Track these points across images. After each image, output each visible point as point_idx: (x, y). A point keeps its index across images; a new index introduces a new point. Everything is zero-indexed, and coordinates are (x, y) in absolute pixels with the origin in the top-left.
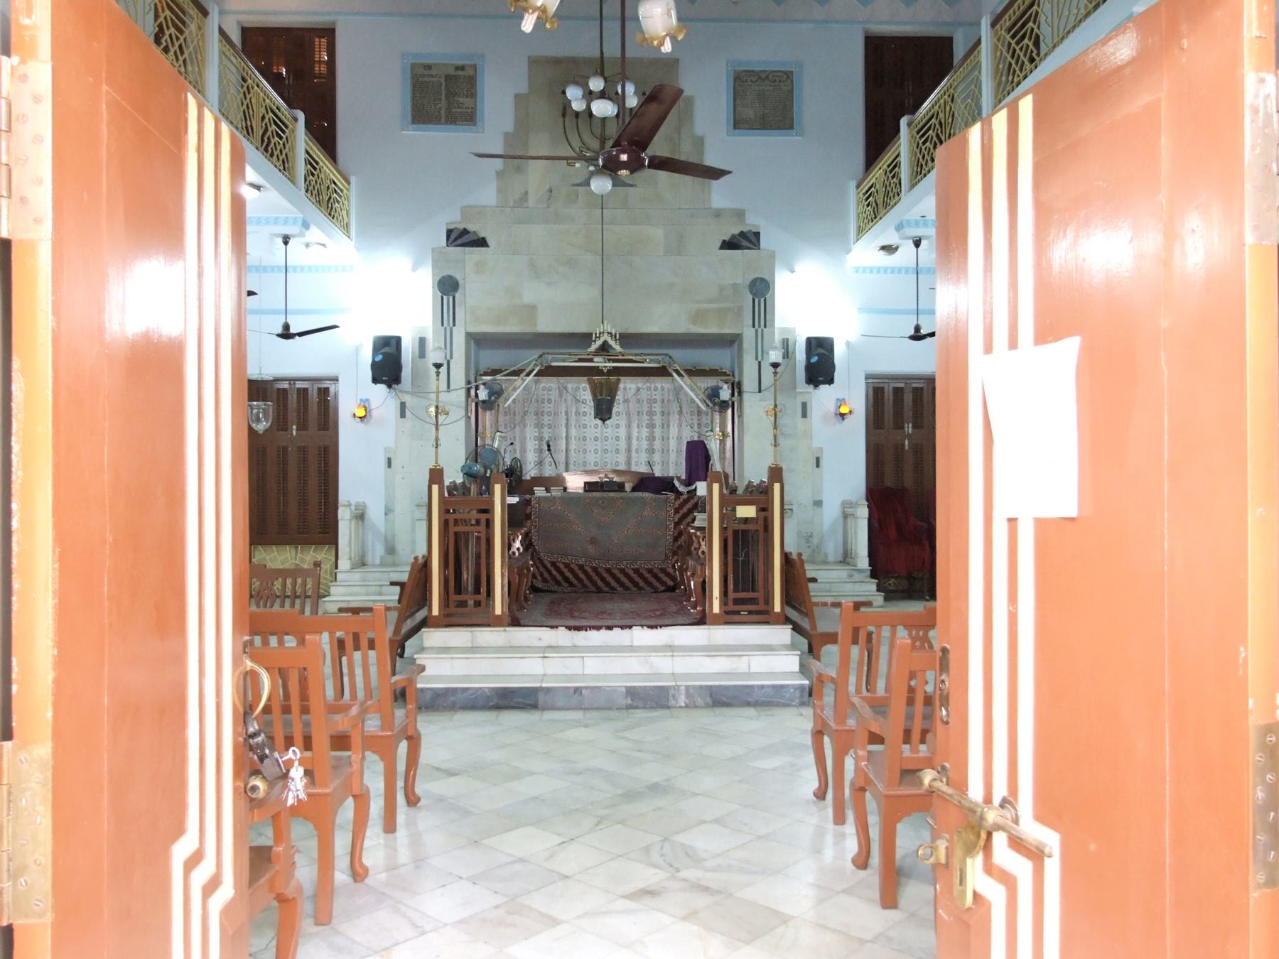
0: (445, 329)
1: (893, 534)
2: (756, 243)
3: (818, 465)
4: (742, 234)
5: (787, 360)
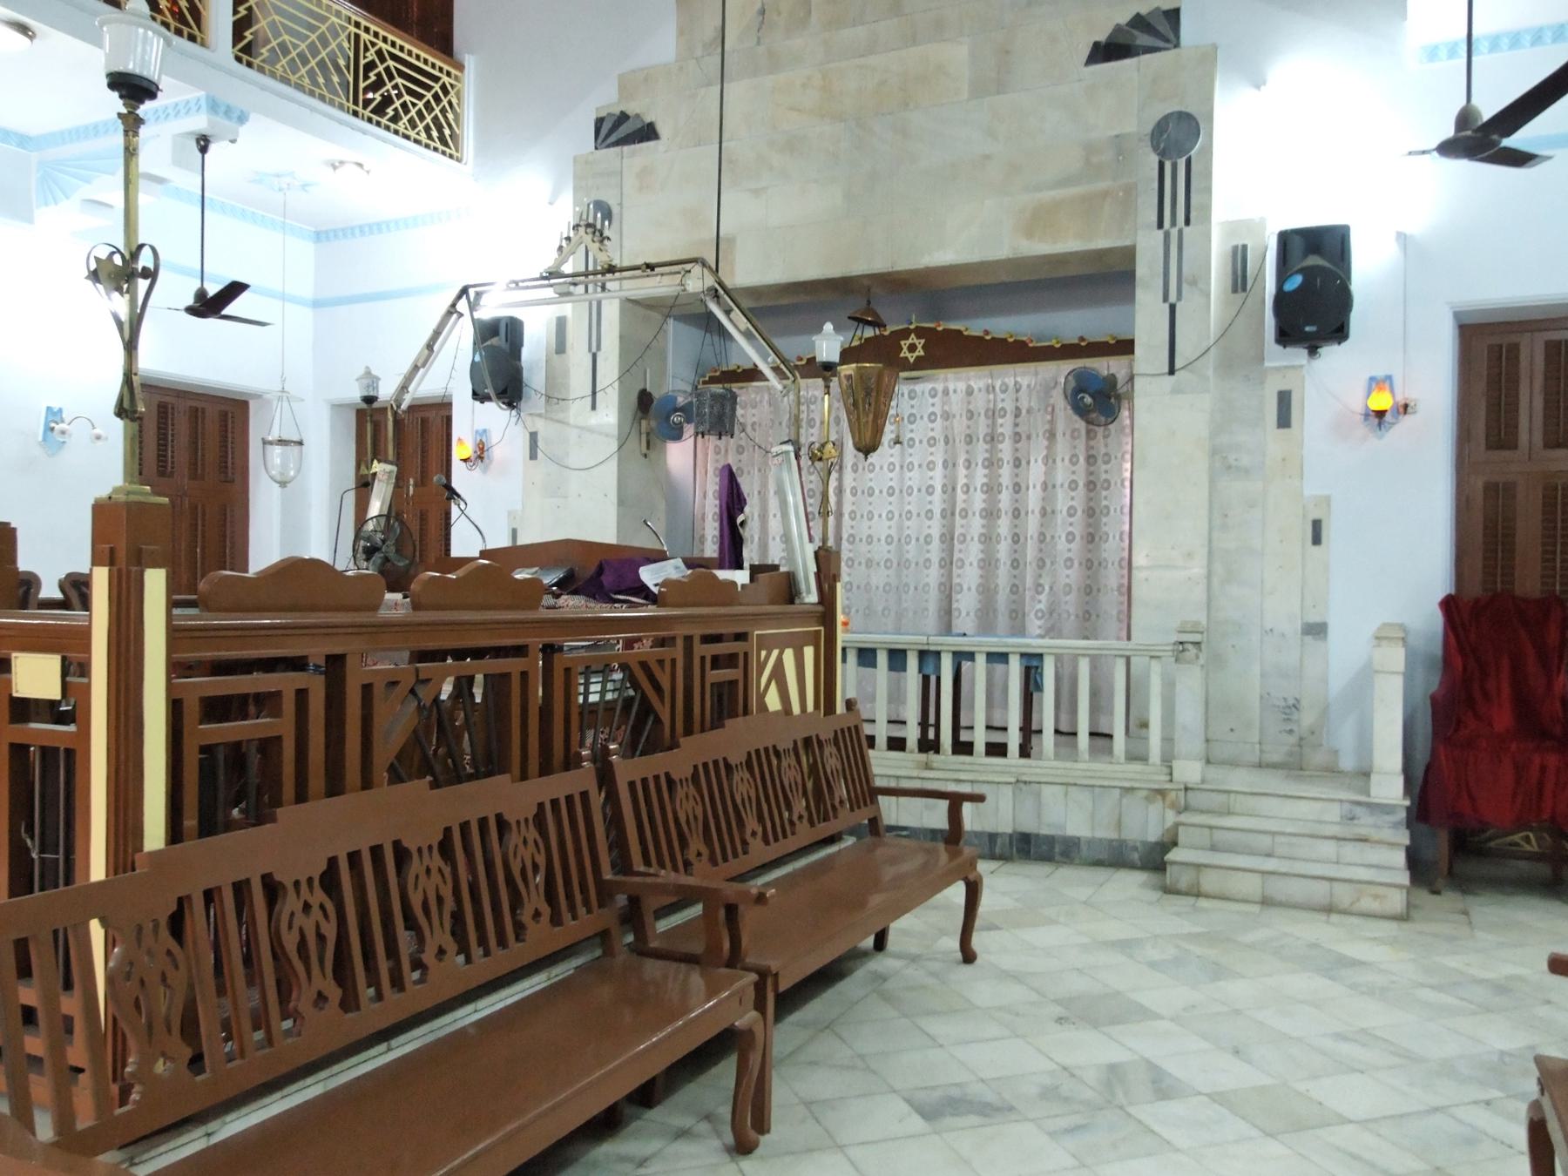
1: (1503, 718)
2: (1172, 37)
3: (1317, 540)
4: (1139, 22)
5: (1244, 295)
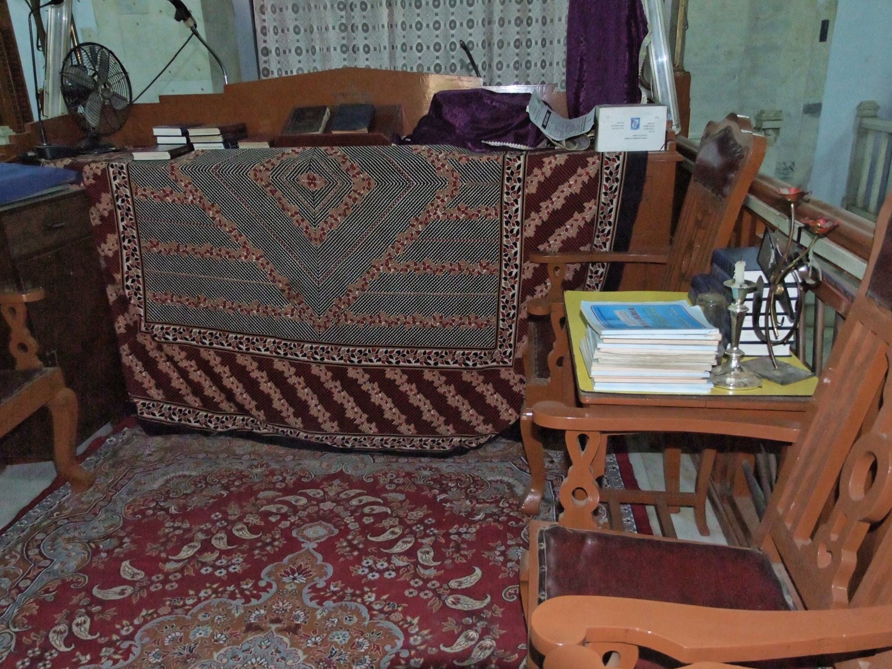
3: (823, 37)
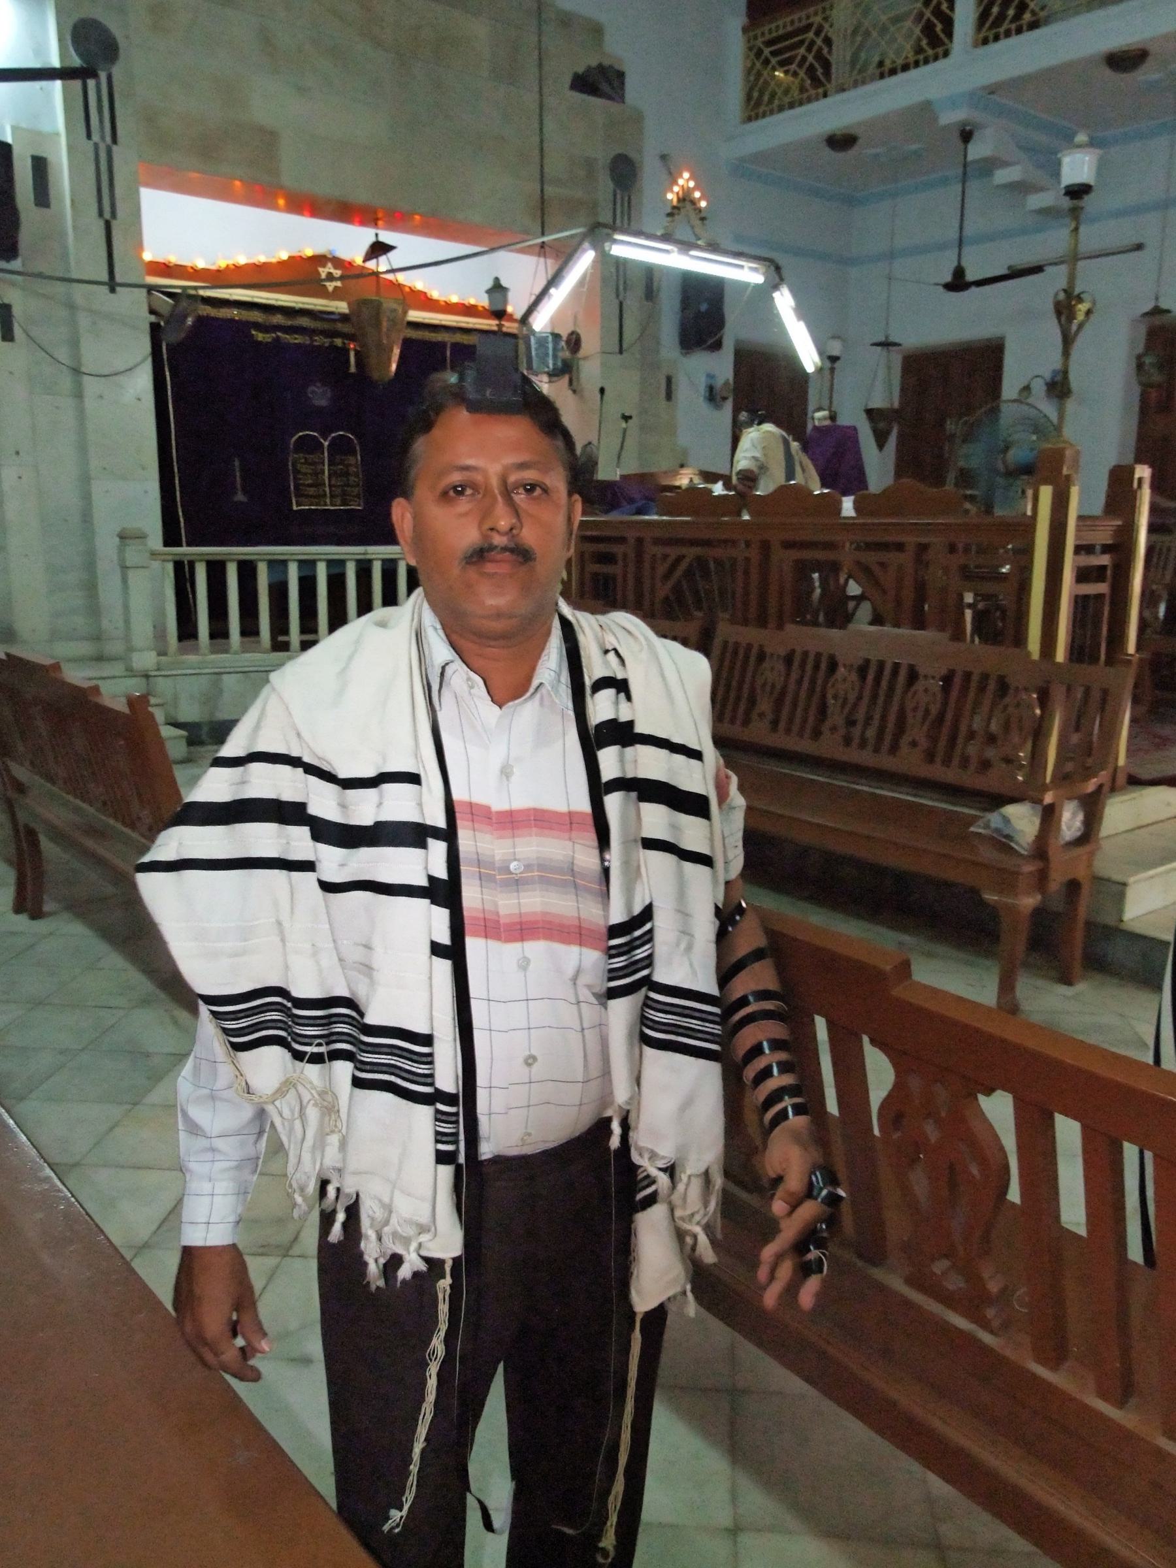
0: (96, 146)
